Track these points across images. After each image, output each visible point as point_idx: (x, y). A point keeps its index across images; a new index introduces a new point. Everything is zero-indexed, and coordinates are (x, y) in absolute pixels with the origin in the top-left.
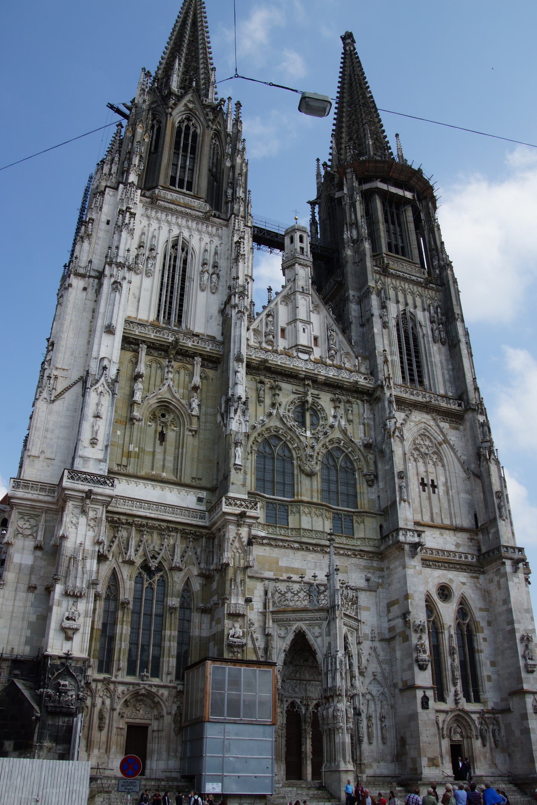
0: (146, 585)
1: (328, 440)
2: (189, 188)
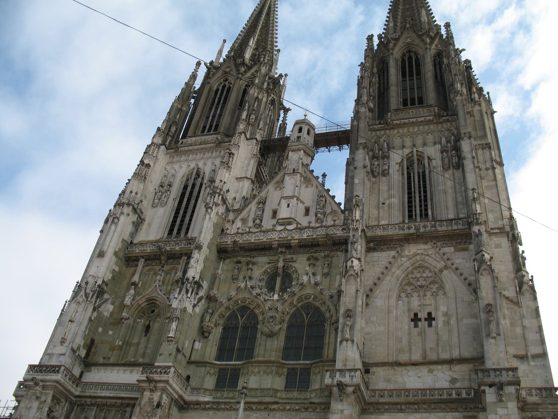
1: (296, 298)
2: (216, 129)
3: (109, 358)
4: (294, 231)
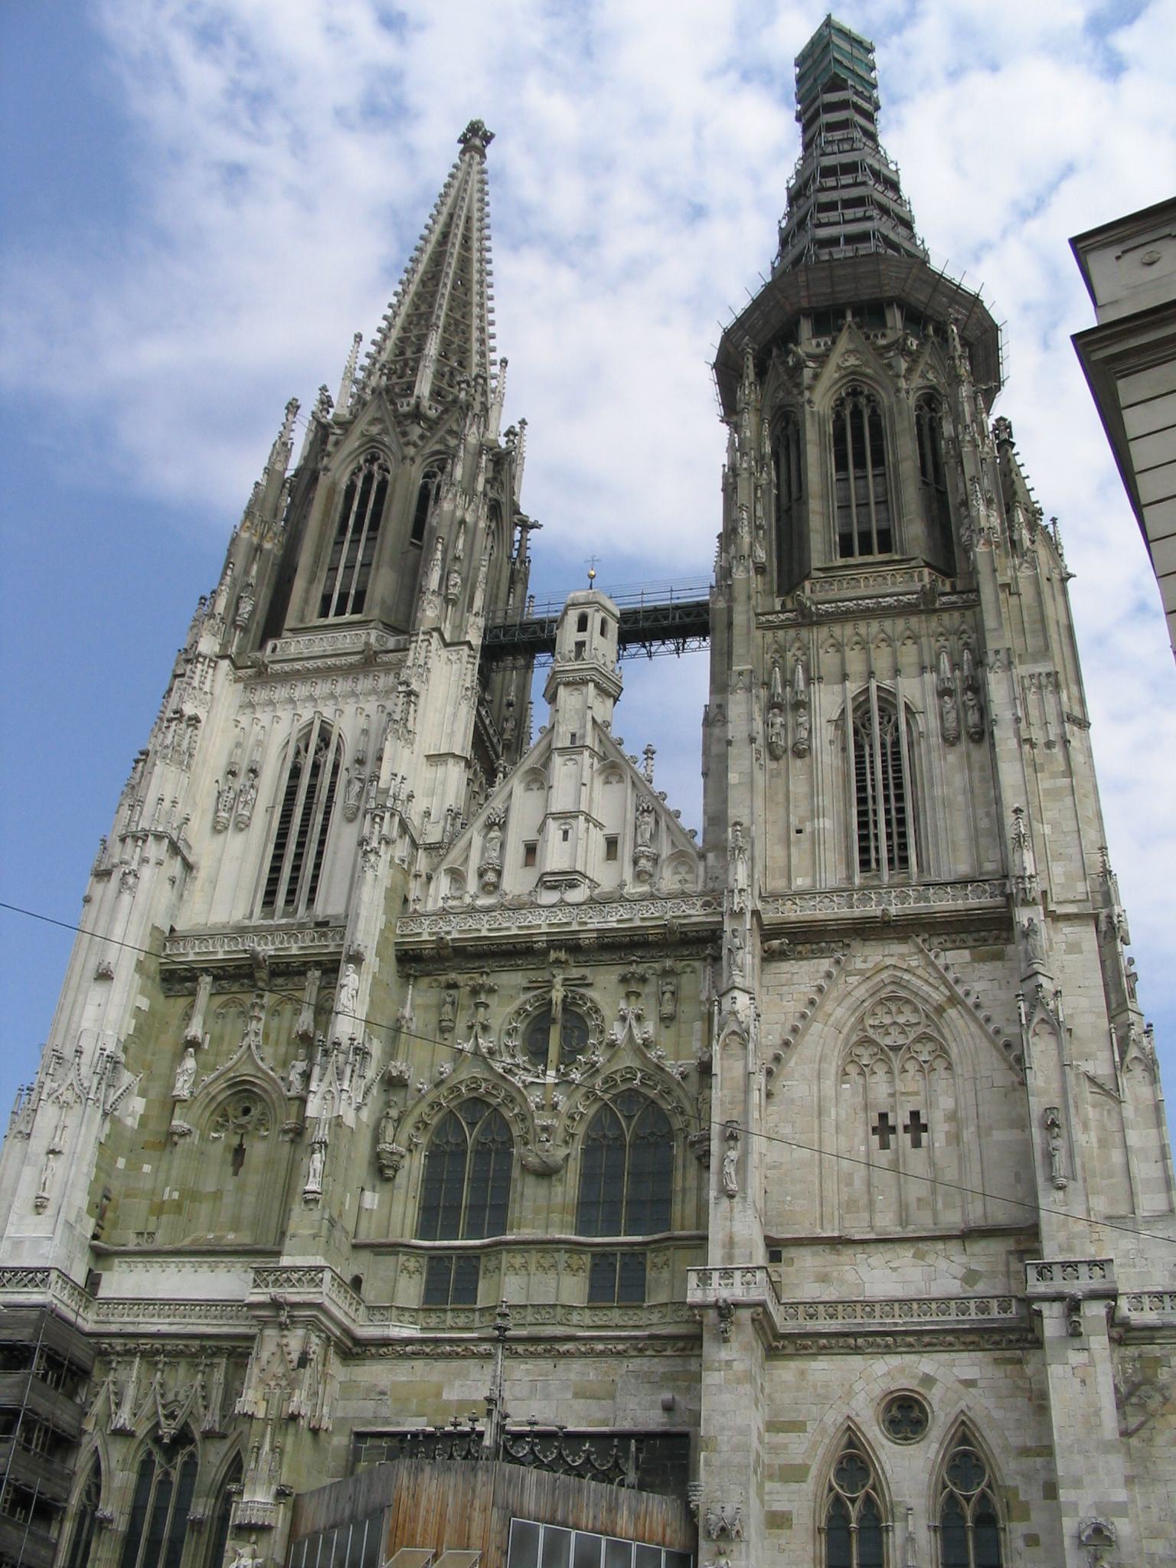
2: (357, 609)
3: (151, 1234)
4: (584, 907)
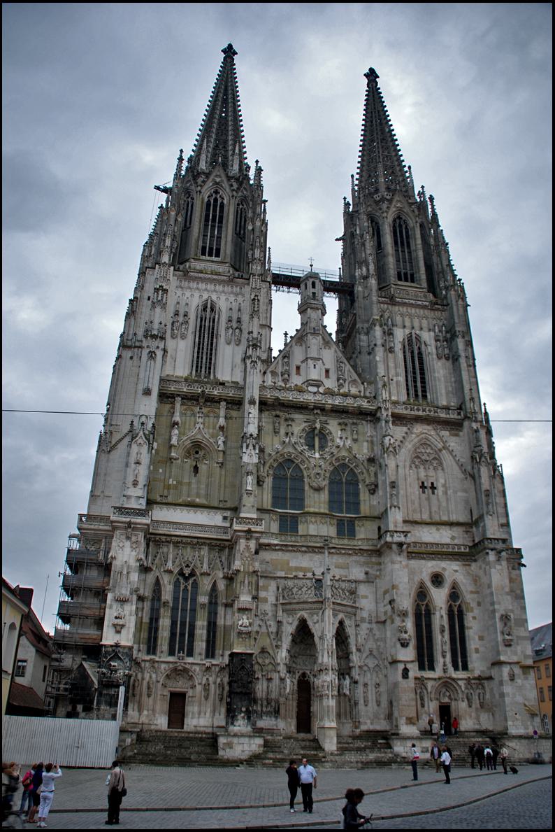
0: (182, 587)
1: (334, 458)
2: (218, 255)
